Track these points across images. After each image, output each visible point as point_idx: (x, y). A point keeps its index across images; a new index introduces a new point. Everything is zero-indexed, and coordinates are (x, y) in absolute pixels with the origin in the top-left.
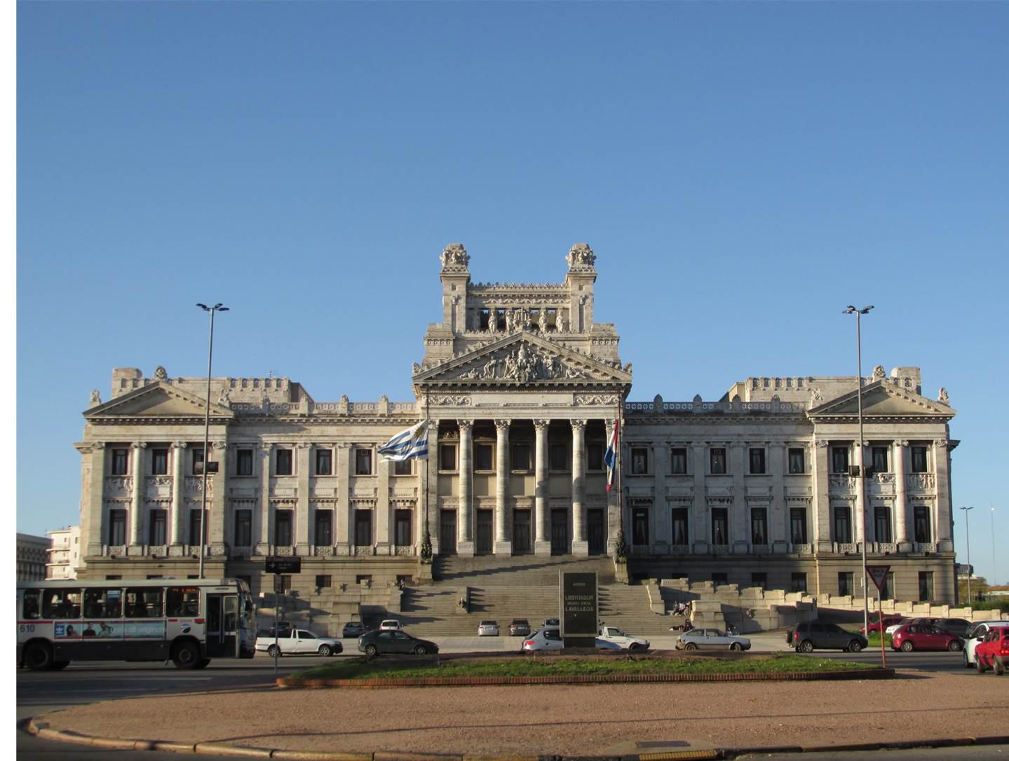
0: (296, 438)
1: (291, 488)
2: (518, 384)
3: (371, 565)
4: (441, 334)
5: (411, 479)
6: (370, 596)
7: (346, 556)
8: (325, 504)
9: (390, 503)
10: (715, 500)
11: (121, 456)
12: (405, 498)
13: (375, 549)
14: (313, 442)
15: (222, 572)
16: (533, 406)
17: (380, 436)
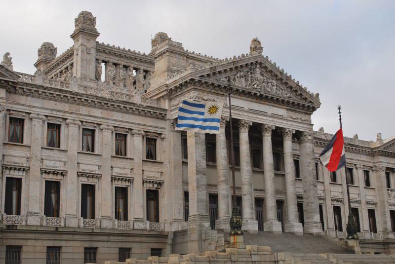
0: (67, 114)
1: (61, 161)
2: (259, 94)
3: (131, 239)
4: (178, 49)
5: (158, 165)
7: (110, 229)
8: (90, 179)
9: (143, 182)
12: (155, 180)
13: (134, 223)
14: (81, 120)
16: (264, 114)
17: (135, 124)
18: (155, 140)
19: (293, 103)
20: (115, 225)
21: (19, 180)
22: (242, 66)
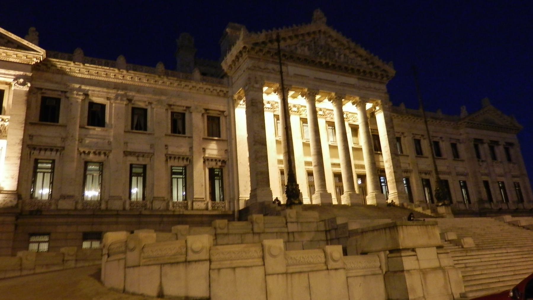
6: (300, 233)
8: (141, 159)
9: (204, 162)
10: (423, 173)
15: (12, 228)
18: (219, 118)
19: (364, 72)
20: (169, 205)
22: (303, 35)
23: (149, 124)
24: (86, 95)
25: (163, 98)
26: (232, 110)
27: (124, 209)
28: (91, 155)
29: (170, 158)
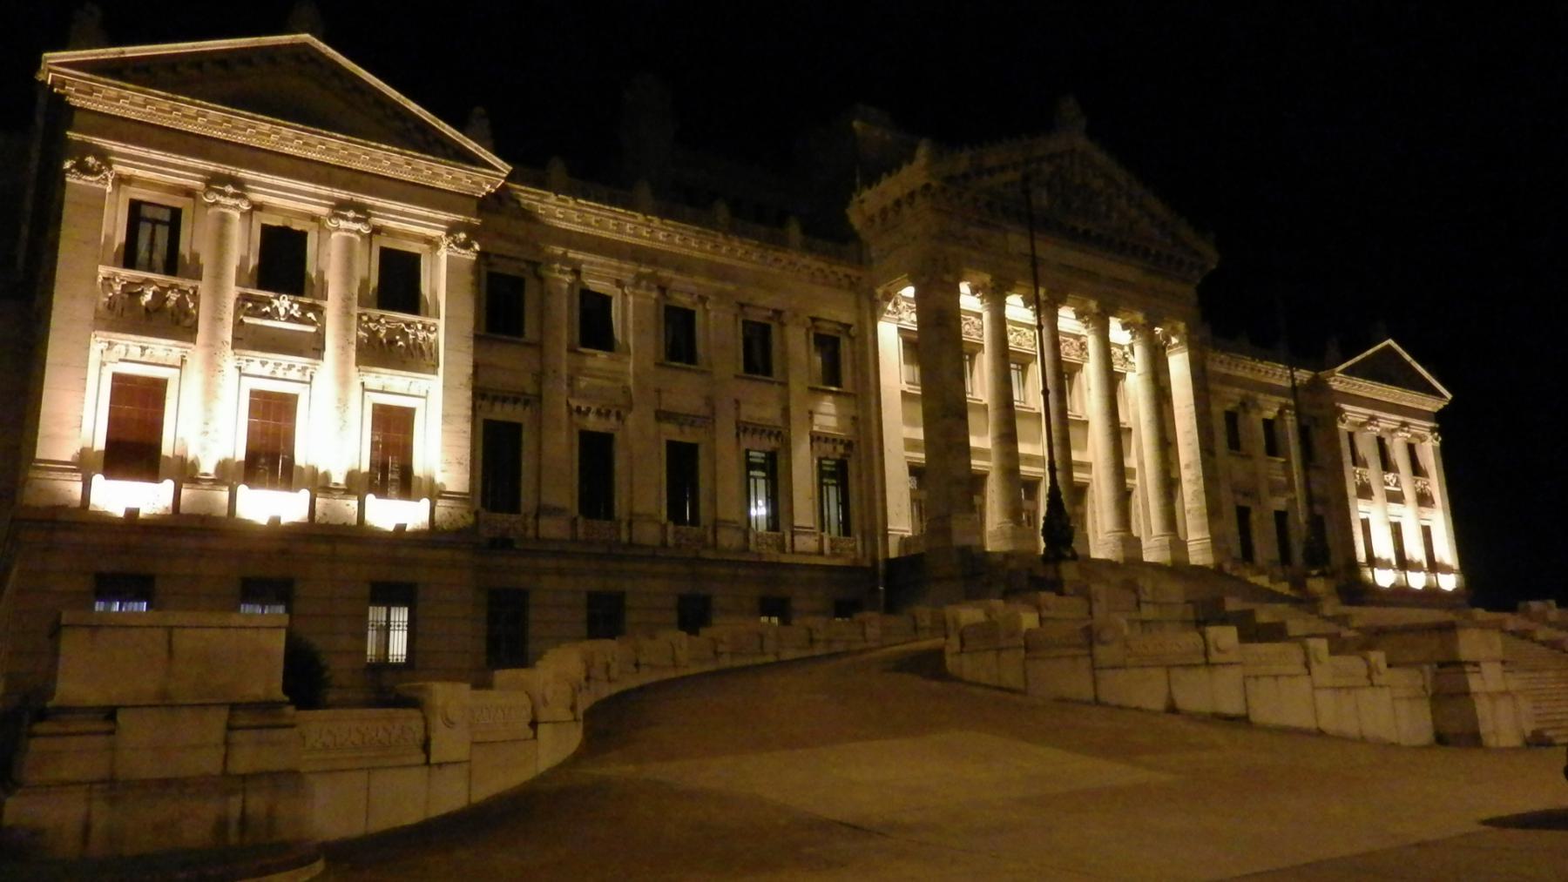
8: (687, 429)
9: (812, 441)
11: (155, 222)
21: (514, 429)
23: (700, 349)
24: (577, 272)
25: (730, 287)
26: (869, 326)
27: (664, 544)
28: (592, 417)
29: (745, 430)
